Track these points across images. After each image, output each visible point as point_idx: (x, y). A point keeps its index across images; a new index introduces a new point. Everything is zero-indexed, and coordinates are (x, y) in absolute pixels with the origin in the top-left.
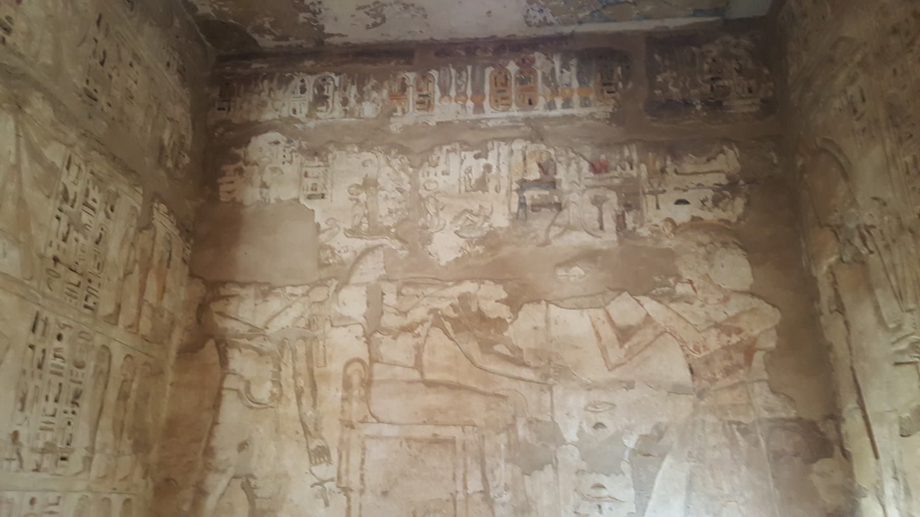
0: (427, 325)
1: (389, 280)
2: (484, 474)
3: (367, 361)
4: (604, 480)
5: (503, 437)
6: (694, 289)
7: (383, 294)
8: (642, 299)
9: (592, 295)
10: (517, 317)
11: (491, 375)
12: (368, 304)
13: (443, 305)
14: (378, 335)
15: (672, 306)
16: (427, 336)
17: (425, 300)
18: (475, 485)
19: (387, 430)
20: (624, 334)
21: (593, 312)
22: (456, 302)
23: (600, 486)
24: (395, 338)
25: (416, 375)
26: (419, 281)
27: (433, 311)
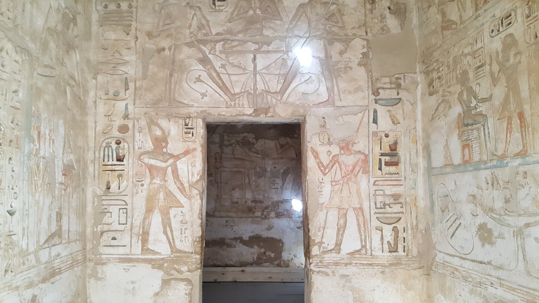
5: (253, 171)
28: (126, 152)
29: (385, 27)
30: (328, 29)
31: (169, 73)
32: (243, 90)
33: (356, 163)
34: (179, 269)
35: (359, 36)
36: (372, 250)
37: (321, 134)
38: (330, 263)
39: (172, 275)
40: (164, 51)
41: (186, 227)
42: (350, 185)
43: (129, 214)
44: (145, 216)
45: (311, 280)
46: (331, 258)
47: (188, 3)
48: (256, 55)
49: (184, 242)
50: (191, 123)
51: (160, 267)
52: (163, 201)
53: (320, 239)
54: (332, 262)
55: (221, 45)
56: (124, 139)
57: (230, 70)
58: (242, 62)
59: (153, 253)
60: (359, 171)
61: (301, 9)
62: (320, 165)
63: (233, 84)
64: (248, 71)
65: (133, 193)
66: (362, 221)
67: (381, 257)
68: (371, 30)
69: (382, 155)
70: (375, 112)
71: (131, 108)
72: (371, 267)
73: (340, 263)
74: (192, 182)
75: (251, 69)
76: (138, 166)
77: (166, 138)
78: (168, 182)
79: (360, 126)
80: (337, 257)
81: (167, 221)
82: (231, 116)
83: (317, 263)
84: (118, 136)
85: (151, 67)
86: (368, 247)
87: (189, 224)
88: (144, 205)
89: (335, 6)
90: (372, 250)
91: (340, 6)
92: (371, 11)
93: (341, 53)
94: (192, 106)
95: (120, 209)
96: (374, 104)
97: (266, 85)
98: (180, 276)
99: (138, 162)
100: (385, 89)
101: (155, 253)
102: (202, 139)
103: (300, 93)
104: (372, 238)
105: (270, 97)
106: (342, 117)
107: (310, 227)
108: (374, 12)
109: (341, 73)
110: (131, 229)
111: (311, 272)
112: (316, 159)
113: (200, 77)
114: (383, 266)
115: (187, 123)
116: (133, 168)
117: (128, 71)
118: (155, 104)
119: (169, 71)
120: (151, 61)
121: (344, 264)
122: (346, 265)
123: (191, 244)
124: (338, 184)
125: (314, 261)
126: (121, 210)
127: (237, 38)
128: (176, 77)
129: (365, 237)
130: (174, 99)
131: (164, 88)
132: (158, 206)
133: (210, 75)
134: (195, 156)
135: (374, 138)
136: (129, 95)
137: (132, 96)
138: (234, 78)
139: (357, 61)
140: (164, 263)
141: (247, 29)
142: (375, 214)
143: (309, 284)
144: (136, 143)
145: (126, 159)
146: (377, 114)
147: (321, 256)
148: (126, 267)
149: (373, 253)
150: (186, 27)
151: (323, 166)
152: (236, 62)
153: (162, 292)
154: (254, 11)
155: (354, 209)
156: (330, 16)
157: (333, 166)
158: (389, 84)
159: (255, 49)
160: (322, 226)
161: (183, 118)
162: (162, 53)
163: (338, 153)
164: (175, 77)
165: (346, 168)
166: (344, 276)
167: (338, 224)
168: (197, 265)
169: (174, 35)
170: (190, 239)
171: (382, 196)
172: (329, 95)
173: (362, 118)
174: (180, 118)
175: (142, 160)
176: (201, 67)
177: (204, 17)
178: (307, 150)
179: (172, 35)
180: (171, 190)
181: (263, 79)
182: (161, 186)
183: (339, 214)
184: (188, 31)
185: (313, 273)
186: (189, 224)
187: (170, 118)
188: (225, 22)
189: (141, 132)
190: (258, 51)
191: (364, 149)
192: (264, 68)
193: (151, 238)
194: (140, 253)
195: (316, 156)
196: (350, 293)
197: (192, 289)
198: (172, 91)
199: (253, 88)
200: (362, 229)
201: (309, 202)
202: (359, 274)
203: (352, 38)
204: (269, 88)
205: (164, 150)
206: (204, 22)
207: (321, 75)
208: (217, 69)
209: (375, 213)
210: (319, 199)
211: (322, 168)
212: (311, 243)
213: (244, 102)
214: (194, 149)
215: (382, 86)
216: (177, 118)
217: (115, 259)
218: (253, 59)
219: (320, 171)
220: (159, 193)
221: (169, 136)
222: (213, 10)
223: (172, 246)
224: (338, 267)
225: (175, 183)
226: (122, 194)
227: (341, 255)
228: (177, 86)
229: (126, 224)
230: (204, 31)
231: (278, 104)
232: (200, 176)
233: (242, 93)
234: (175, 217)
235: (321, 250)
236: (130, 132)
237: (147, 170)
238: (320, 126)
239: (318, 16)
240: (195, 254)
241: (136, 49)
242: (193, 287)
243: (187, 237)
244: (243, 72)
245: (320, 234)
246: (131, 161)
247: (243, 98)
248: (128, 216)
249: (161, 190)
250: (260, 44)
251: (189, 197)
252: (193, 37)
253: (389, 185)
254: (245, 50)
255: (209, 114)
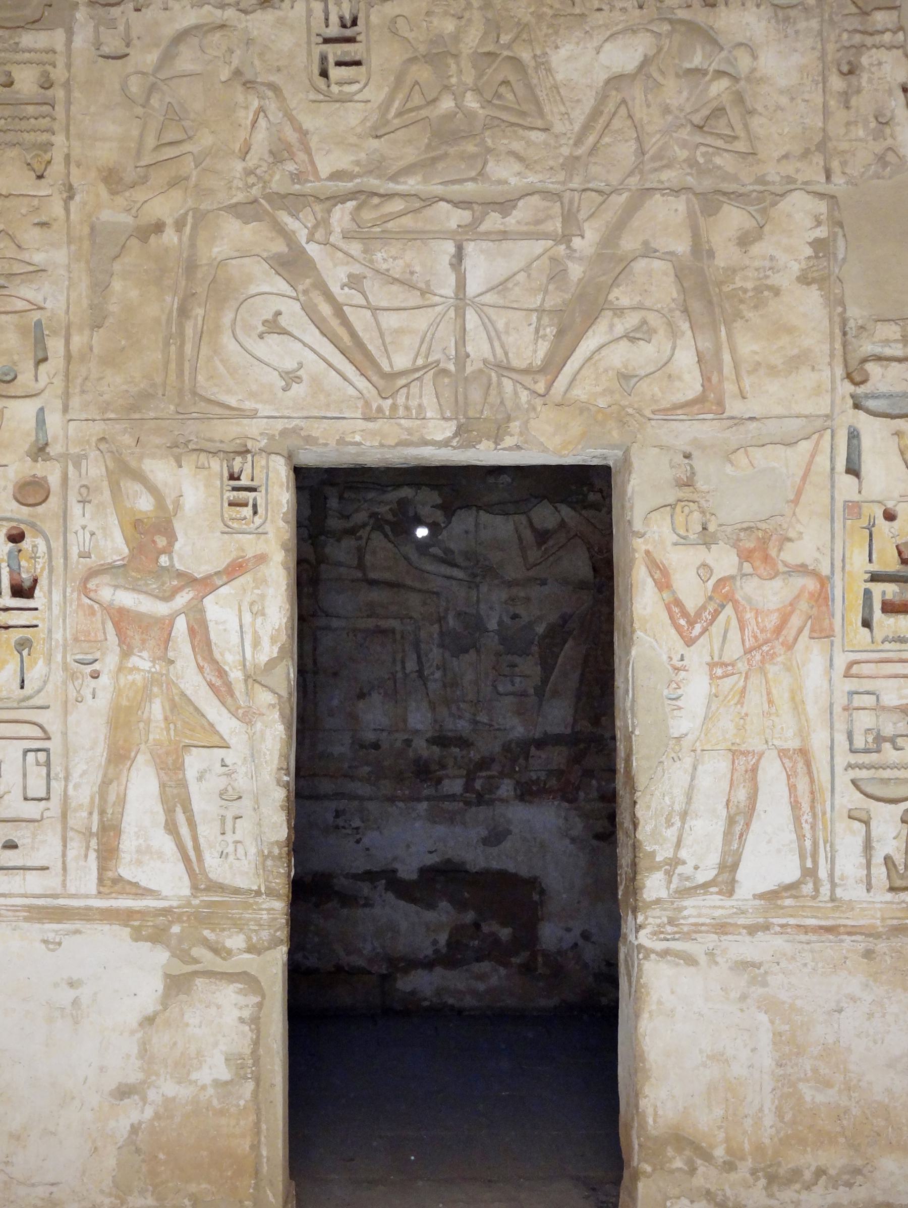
0: (368, 528)
1: (332, 485)
2: (419, 657)
3: (314, 562)
4: (517, 660)
6: (603, 497)
7: (326, 498)
8: (557, 505)
9: (516, 502)
10: (450, 523)
11: (426, 575)
12: (312, 507)
13: (383, 509)
14: (323, 538)
15: (583, 512)
16: (368, 539)
17: (366, 504)
18: (411, 665)
19: (342, 623)
20: (542, 536)
21: (516, 517)
22: (395, 506)
23: (515, 666)
24: (339, 540)
25: (359, 575)
26: (359, 485)
27: (373, 515)
28: (43, 569)
29: (890, 153)
30: (701, 160)
31: (175, 306)
32: (420, 362)
33: (791, 604)
34: (217, 942)
35: (806, 183)
36: (833, 885)
37: (678, 509)
38: (702, 925)
39: (196, 961)
40: (162, 232)
41: (237, 813)
42: (770, 676)
43: (57, 768)
44: (105, 775)
45: (639, 977)
46: (704, 911)
47: (238, 73)
48: (465, 243)
49: (231, 858)
50: (250, 471)
51: (158, 937)
52: (163, 725)
53: (672, 850)
54: (708, 921)
55: (347, 212)
56: (33, 525)
57: (379, 294)
58: (418, 269)
59: (134, 890)
60: (800, 631)
61: (614, 93)
62: (677, 610)
63: (388, 340)
64: (437, 299)
65: (66, 702)
66: (807, 794)
67: (865, 905)
68: (844, 164)
69: (875, 578)
70: (854, 436)
71: (54, 421)
72: (831, 937)
73: (731, 924)
74: (255, 666)
75: (449, 290)
76: (81, 613)
77: (169, 522)
78: (179, 664)
79: (804, 484)
80: (722, 907)
81: (175, 791)
82: (382, 445)
83: (659, 926)
84: (16, 516)
85: (117, 285)
86: (823, 873)
87: (247, 803)
88: (102, 737)
89: (724, 83)
90: (833, 885)
91: (742, 83)
92: (846, 99)
93: (745, 241)
94: (253, 415)
95: (26, 752)
96: (852, 412)
97: (497, 344)
98: (220, 965)
99: (79, 599)
100: (885, 363)
101: (140, 892)
102: (287, 522)
103: (610, 372)
104: (837, 847)
105: (510, 382)
106: (746, 451)
107: (640, 812)
108: (854, 102)
109: (742, 307)
110: (64, 816)
111: (639, 953)
112: (660, 590)
113: (279, 317)
114: (871, 933)
115: (236, 470)
116: (64, 621)
117: (45, 299)
118: (134, 408)
119: (176, 300)
120: (117, 267)
121: (744, 928)
122: (752, 930)
123: (254, 866)
124: (733, 674)
125: (650, 920)
126: (31, 756)
127: (400, 188)
128: (200, 319)
129: (815, 844)
130: (194, 393)
131: (160, 357)
132: (146, 742)
133: (310, 312)
134: (264, 581)
135: (849, 522)
136: (48, 381)
137: (59, 382)
138: (390, 321)
139: (795, 268)
140: (171, 923)
141: (434, 160)
142: (846, 770)
143: (633, 990)
144: (71, 537)
145: (41, 589)
146: (859, 445)
147: (673, 903)
148: (51, 936)
149: (839, 892)
150: (234, 152)
151: (685, 614)
152: (397, 268)
153: (167, 1013)
154: (455, 99)
155: (783, 753)
156: (708, 118)
157: (716, 614)
158: (900, 346)
159: (459, 226)
160: (677, 807)
161: (221, 455)
162: (153, 239)
163: (733, 571)
164: (196, 319)
165: (757, 623)
166: (743, 966)
167: (728, 801)
168: (276, 931)
169: (193, 179)
170: (253, 850)
171: (873, 712)
172: (706, 379)
173: (813, 456)
174: (215, 454)
175: (92, 595)
176: (282, 286)
177: (292, 119)
178: (632, 561)
179: (187, 178)
180: (188, 693)
181: (487, 324)
182: (154, 680)
183: (733, 770)
184: (239, 166)
185: (645, 958)
186: (247, 803)
187: (181, 454)
188: (360, 136)
189: (89, 502)
190: (470, 231)
191: (816, 560)
192: (493, 289)
193: (128, 844)
194: (94, 892)
195: (664, 583)
196: (763, 1018)
197: (260, 1006)
198: (187, 365)
199: (454, 353)
200: (805, 817)
201: (637, 732)
202: (793, 958)
203: (779, 189)
204: (506, 354)
205: (164, 560)
206: (291, 136)
207: (678, 313)
208: (335, 289)
209: (850, 766)
210: (671, 722)
211: (682, 622)
212: (642, 864)
213: (425, 402)
214: (262, 559)
215: (878, 350)
216: (203, 456)
217: (15, 909)
218: (454, 256)
219: (673, 631)
220: (150, 702)
221: (178, 515)
222: (321, 97)
223: (194, 870)
224: (725, 937)
225: (201, 668)
226: (31, 703)
227: (737, 900)
228: (205, 351)
229: (48, 799)
230: (291, 167)
231: (539, 409)
232: (279, 645)
233: (417, 370)
234: (200, 778)
235: (673, 886)
236: (54, 501)
237: (110, 626)
238: (674, 484)
239: (670, 118)
240: (267, 895)
241: (69, 227)
242: (263, 996)
243: (240, 842)
244: (419, 301)
245: (671, 834)
246: (57, 597)
247: (421, 387)
248: (52, 775)
249: (155, 690)
250: (476, 207)
251: (245, 714)
252: (254, 185)
253: (896, 676)
254: (428, 227)
255: (309, 440)
